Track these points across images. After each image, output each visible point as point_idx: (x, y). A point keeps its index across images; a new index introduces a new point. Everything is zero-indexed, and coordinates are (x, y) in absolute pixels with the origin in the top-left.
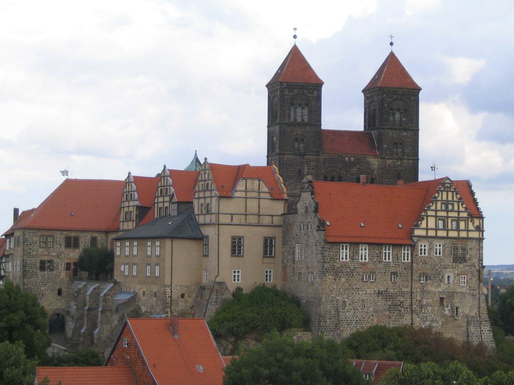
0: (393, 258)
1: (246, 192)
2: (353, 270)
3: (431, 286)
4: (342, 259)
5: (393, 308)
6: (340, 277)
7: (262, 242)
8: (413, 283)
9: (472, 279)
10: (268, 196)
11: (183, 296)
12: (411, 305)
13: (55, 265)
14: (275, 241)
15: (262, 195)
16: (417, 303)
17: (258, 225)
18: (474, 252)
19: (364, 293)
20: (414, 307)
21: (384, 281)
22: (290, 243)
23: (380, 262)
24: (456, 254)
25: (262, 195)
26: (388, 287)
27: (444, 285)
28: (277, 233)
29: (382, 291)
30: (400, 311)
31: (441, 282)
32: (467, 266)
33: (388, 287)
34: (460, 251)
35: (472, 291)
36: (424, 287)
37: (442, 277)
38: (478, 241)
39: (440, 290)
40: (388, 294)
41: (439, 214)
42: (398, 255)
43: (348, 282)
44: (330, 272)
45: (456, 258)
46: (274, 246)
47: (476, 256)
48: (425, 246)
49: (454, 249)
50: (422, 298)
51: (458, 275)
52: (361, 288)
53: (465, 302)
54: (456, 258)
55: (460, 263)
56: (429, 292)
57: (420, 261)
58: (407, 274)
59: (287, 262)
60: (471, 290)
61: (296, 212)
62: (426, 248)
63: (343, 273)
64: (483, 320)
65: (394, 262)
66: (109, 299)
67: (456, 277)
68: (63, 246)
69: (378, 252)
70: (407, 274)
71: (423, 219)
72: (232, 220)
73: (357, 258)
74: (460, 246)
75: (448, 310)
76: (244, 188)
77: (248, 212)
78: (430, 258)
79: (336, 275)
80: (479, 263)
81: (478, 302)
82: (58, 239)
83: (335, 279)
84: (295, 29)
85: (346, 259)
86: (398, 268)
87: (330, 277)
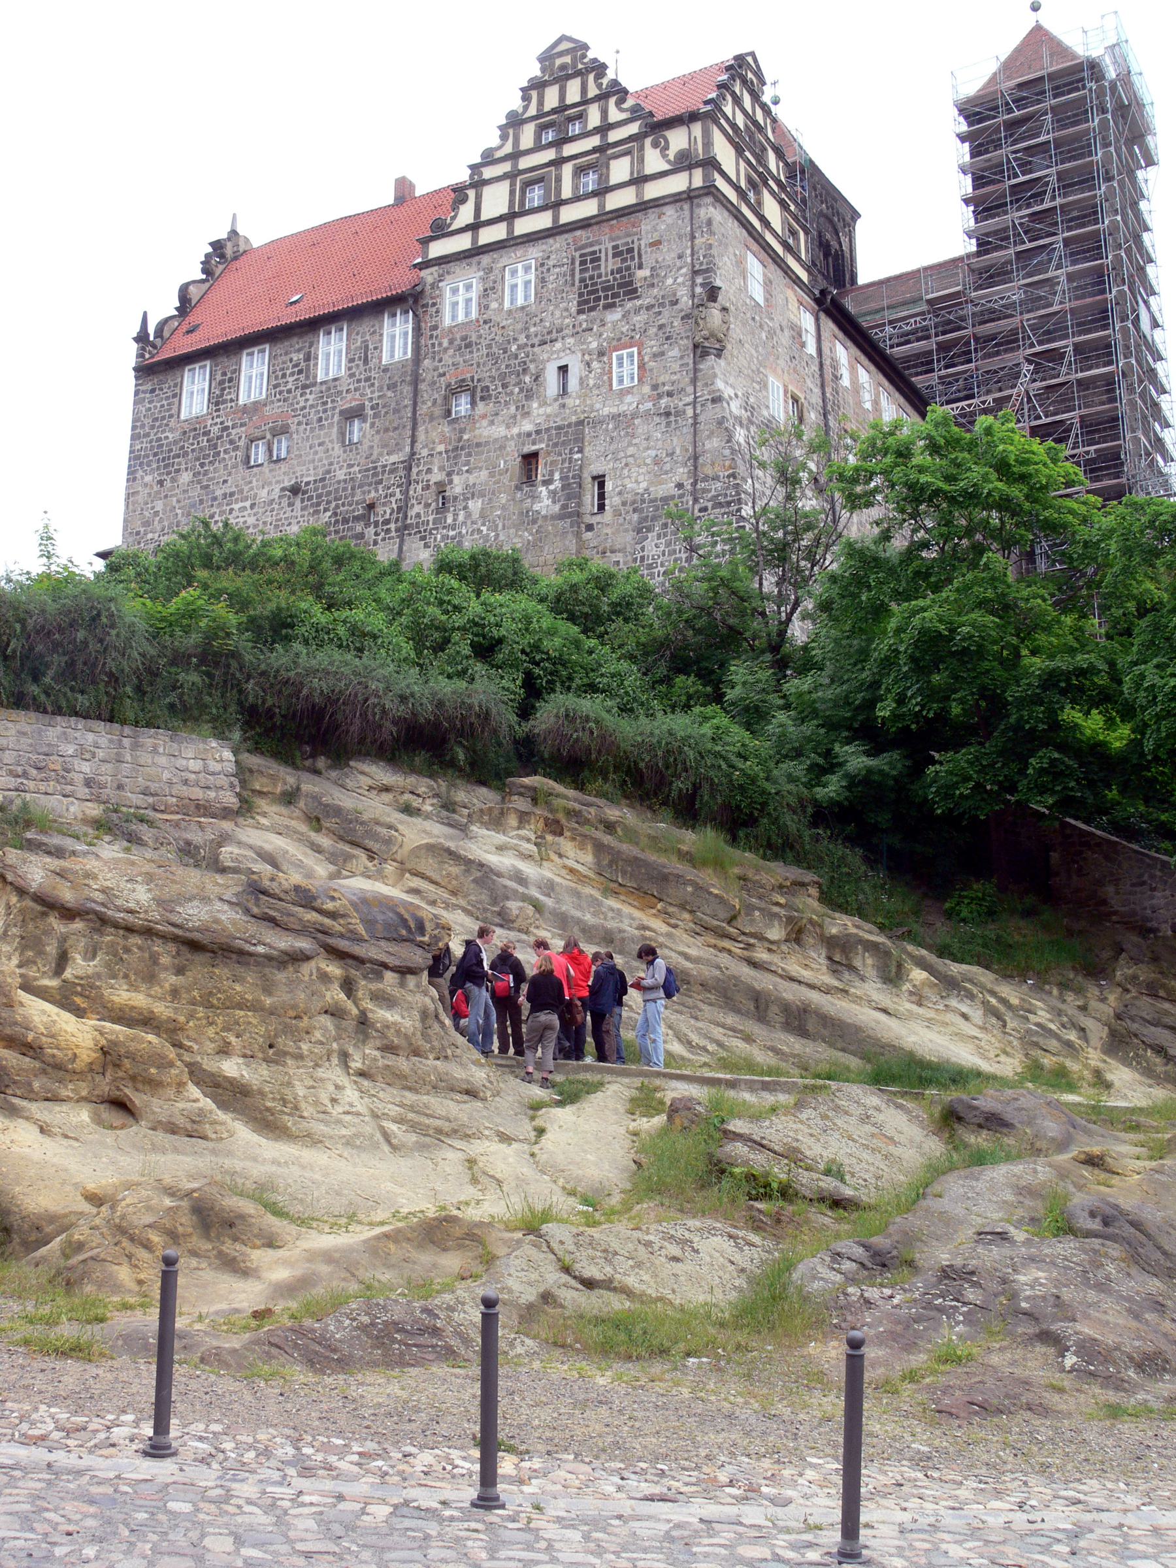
0: (351, 360)
2: (219, 438)
3: (492, 423)
5: (336, 532)
6: (178, 471)
9: (662, 354)
12: (403, 509)
16: (430, 496)
18: (667, 255)
19: (248, 504)
20: (412, 513)
23: (305, 387)
24: (592, 278)
26: (331, 464)
27: (540, 406)
29: (308, 483)
30: (361, 536)
31: (528, 397)
32: (637, 311)
33: (331, 464)
34: (609, 265)
35: (664, 401)
36: (462, 431)
38: (686, 206)
39: (528, 426)
40: (324, 487)
41: (525, 163)
42: (367, 347)
43: (199, 482)
45: (590, 293)
47: (678, 263)
48: (468, 288)
49: (583, 263)
50: (449, 474)
51: (601, 354)
52: (241, 491)
53: (631, 451)
54: (590, 293)
56: (478, 445)
57: (445, 343)
60: (660, 396)
62: (474, 294)
64: (710, 505)
65: (352, 375)
67: (595, 365)
70: (398, 403)
71: (464, 200)
73: (233, 396)
75: (553, 494)
78: (485, 322)
79: (166, 466)
80: (693, 285)
81: (690, 437)
83: (161, 483)
86: (368, 391)
87: (148, 479)
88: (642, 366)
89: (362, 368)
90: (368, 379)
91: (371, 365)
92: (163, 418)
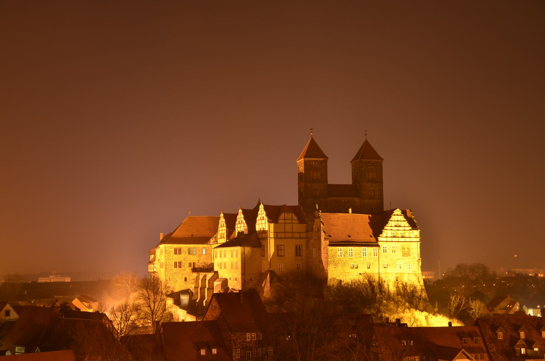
0: (368, 255)
1: (285, 219)
2: (346, 262)
4: (339, 256)
7: (294, 248)
8: (380, 269)
10: (297, 222)
11: (251, 280)
13: (183, 264)
14: (302, 246)
15: (294, 222)
17: (292, 238)
19: (352, 275)
21: (363, 268)
22: (310, 248)
25: (294, 222)
28: (303, 242)
34: (406, 250)
37: (397, 265)
43: (342, 269)
44: (332, 264)
45: (404, 254)
46: (302, 250)
49: (403, 249)
51: (406, 263)
55: (406, 257)
57: (383, 256)
58: (376, 264)
59: (309, 258)
61: (312, 230)
63: (339, 264)
65: (368, 257)
66: (211, 282)
68: (187, 253)
69: (359, 251)
72: (277, 236)
74: (406, 247)
76: (283, 218)
77: (286, 231)
79: (336, 265)
82: (184, 250)
83: (335, 268)
84: (312, 129)
85: (341, 256)
87: (332, 266)
88: (411, 267)
89: (370, 256)
90: (371, 259)
91: (372, 256)
92: (334, 256)
